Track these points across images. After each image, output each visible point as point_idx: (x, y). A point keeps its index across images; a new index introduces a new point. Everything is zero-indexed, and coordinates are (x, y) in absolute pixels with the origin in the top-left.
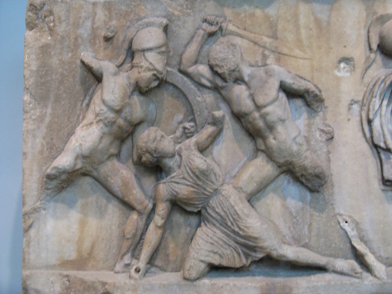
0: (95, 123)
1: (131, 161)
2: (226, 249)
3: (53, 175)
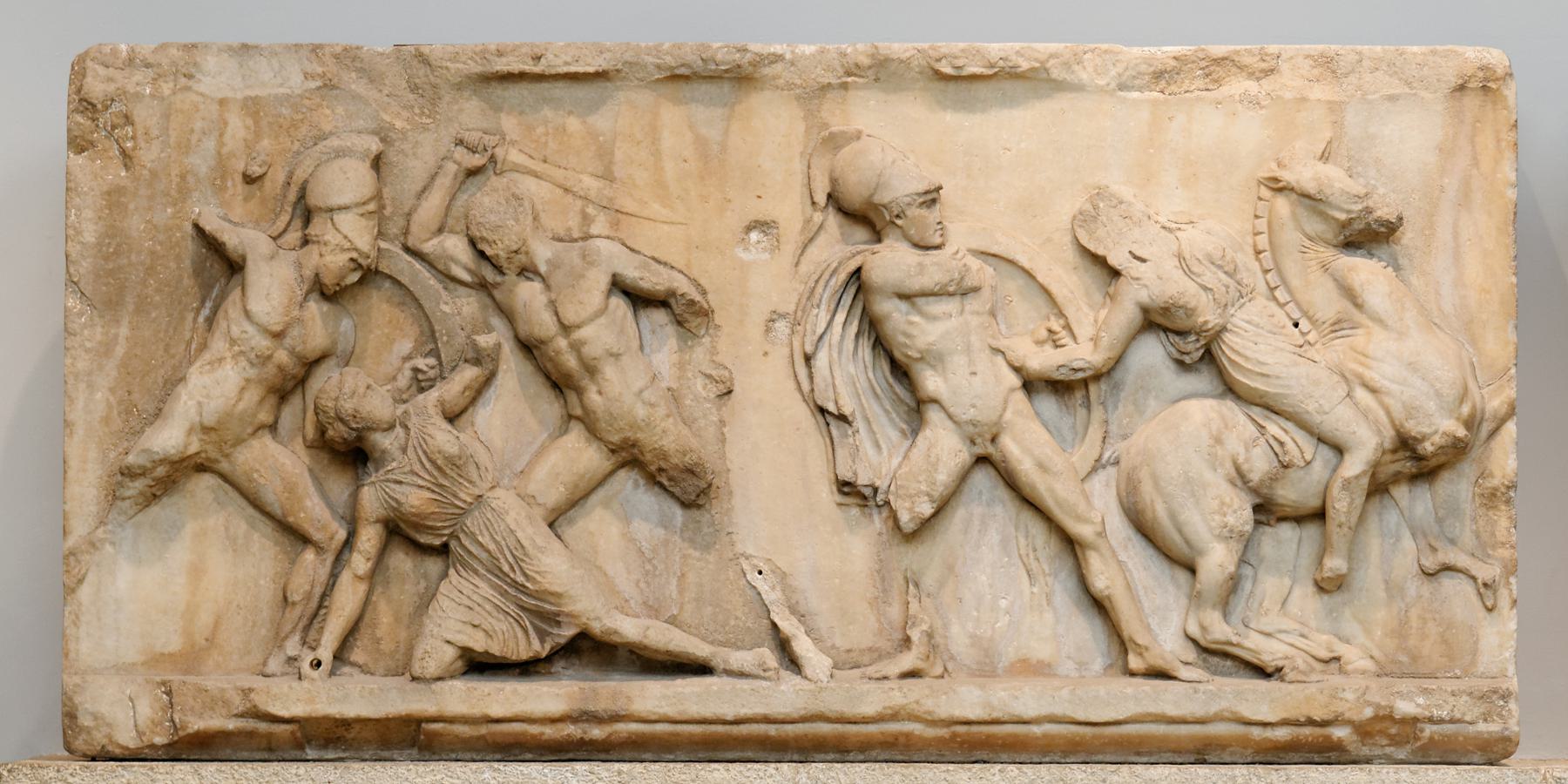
0: (229, 360)
1: (300, 440)
2: (499, 620)
3: (139, 467)
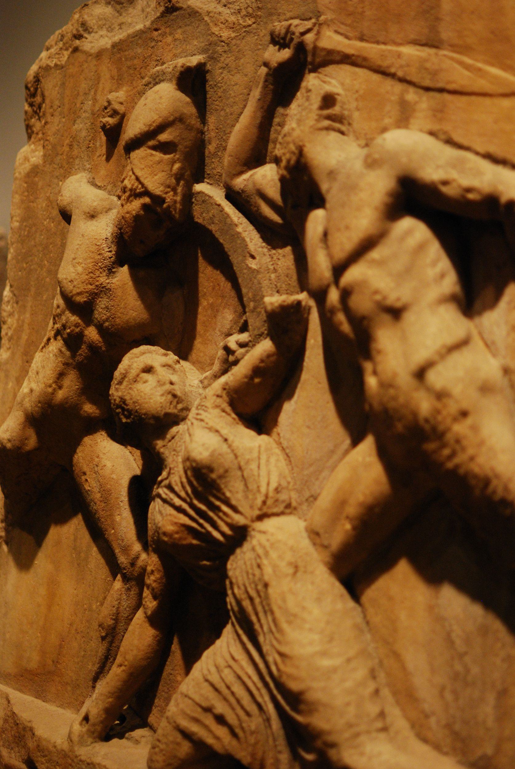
2: (248, 714)
